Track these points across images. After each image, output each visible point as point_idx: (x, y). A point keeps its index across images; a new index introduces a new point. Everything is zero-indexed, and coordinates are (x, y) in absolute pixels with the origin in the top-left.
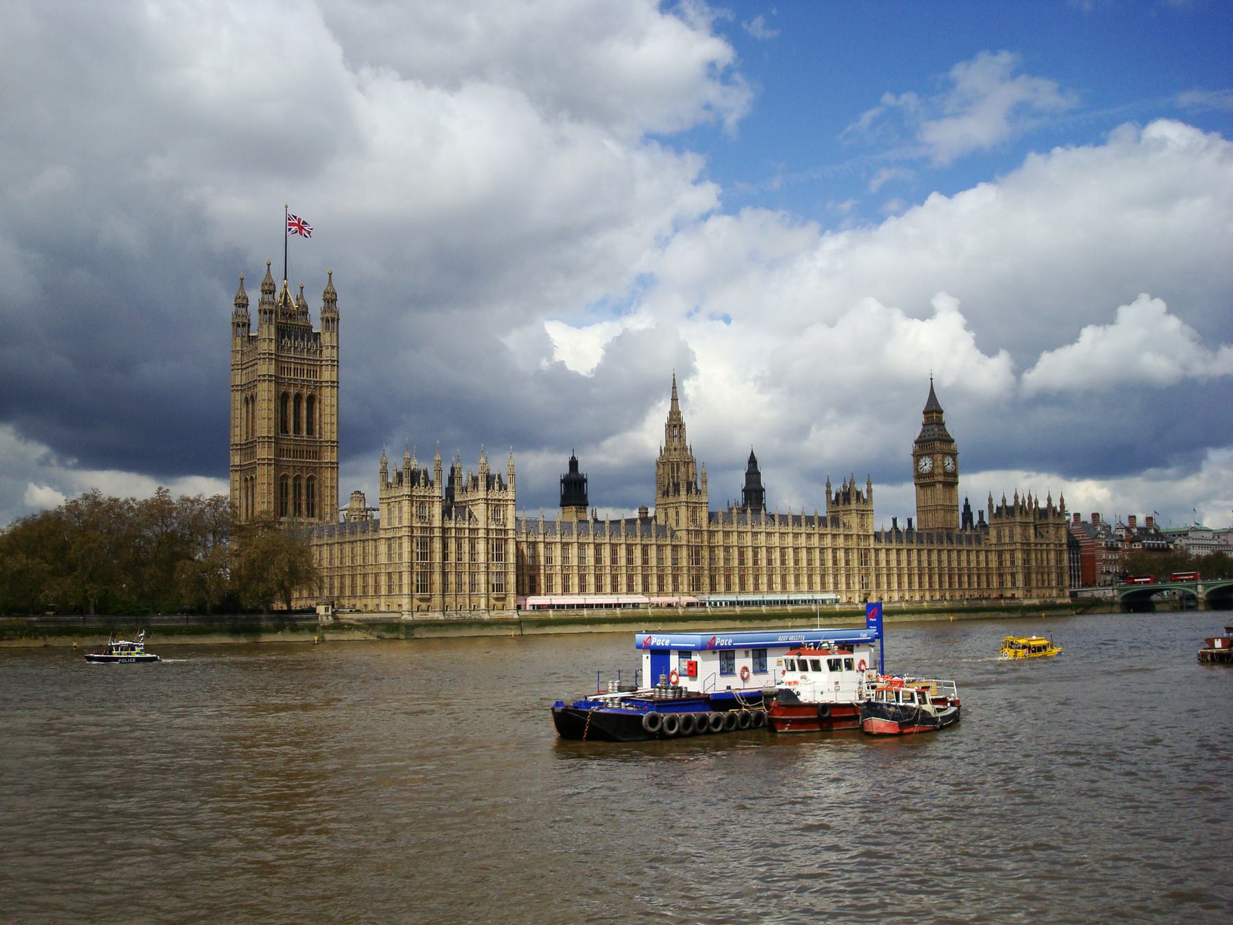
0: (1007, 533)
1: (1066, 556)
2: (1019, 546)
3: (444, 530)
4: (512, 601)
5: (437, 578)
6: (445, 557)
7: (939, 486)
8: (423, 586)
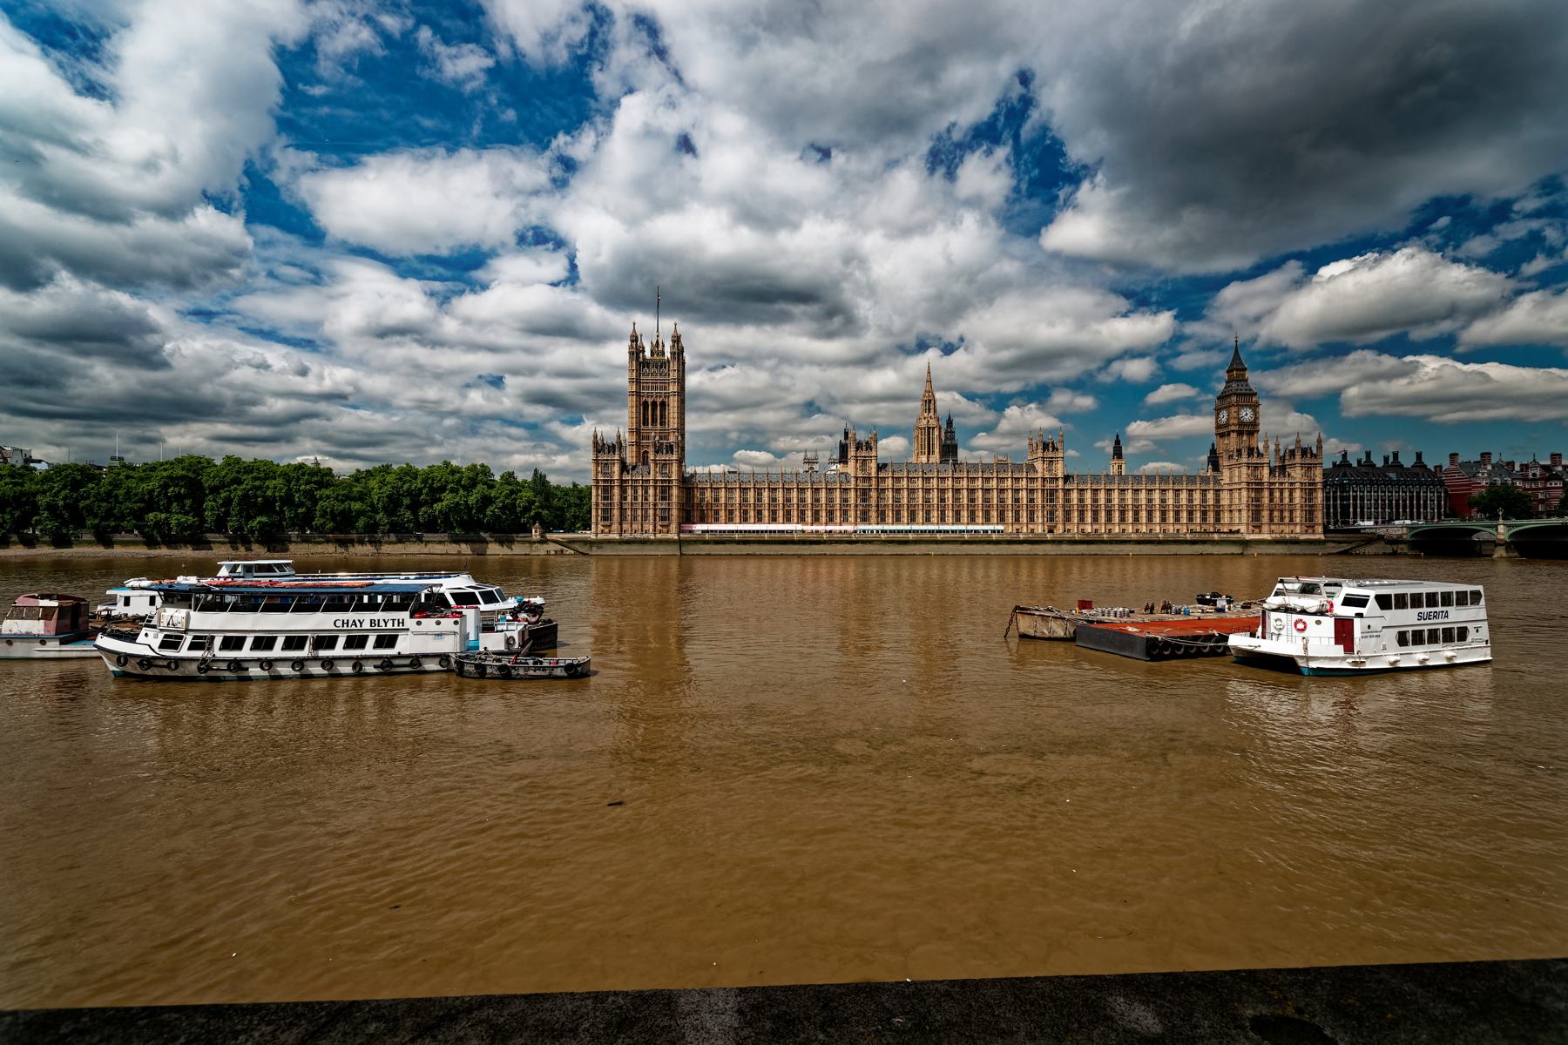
1: (1320, 495)
3: (622, 481)
4: (674, 527)
5: (616, 512)
6: (623, 497)
7: (1233, 435)
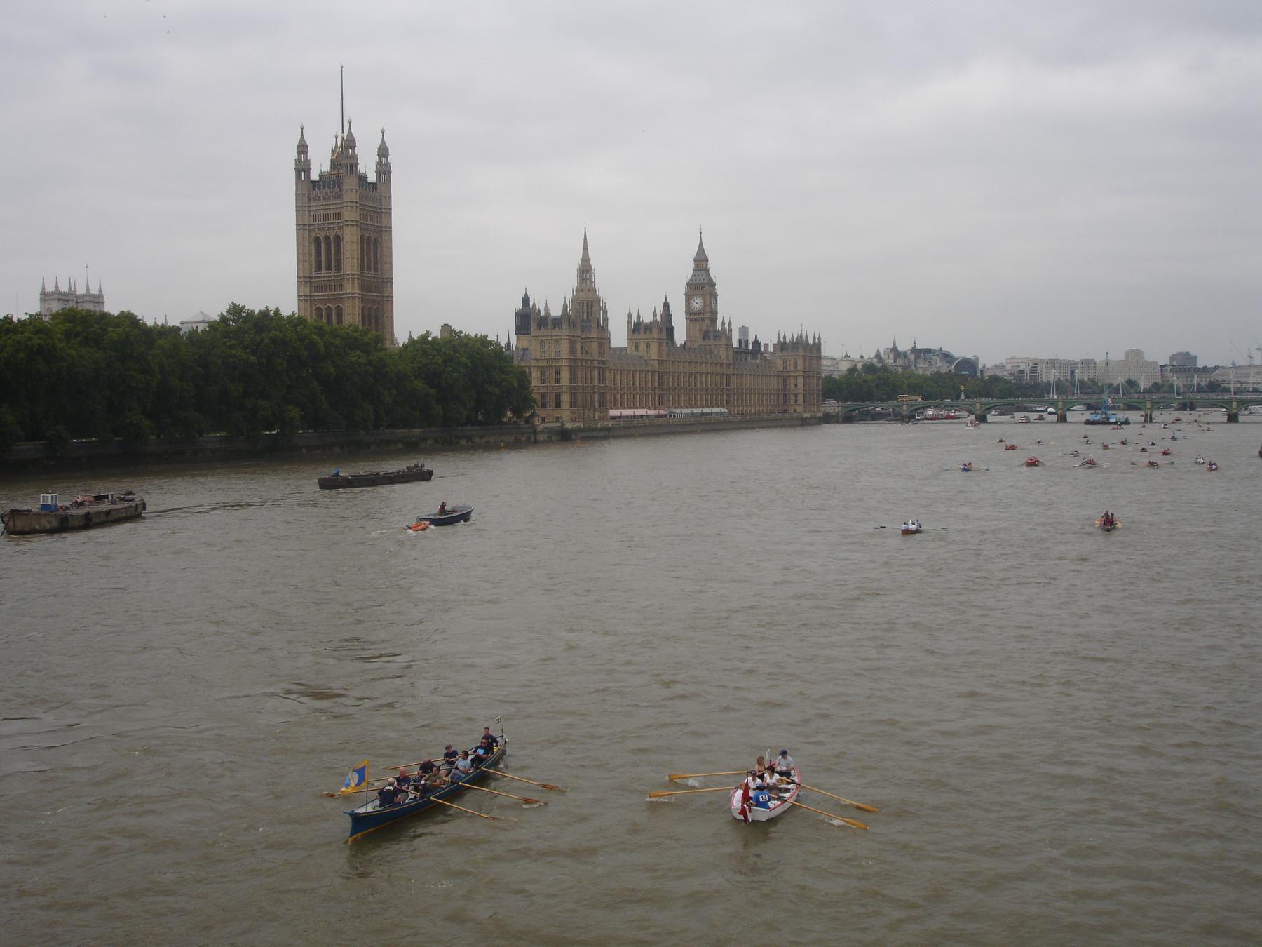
0: (792, 362)
2: (801, 374)
8: (572, 404)
